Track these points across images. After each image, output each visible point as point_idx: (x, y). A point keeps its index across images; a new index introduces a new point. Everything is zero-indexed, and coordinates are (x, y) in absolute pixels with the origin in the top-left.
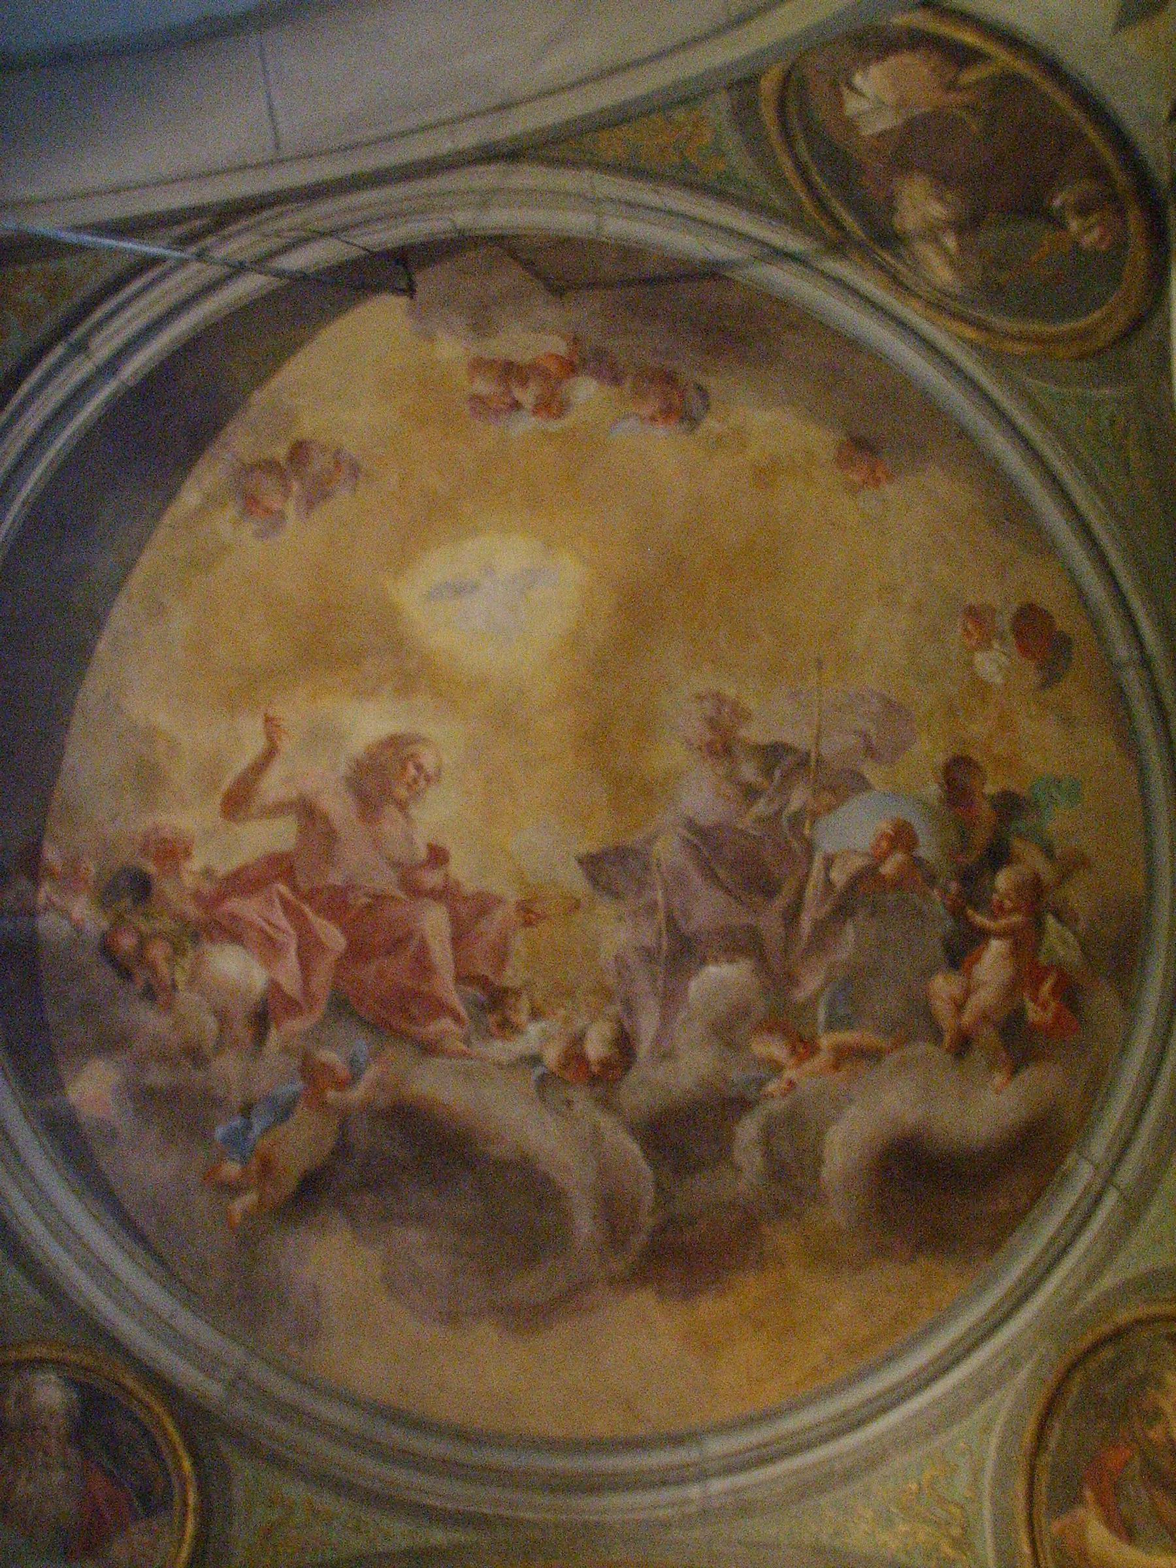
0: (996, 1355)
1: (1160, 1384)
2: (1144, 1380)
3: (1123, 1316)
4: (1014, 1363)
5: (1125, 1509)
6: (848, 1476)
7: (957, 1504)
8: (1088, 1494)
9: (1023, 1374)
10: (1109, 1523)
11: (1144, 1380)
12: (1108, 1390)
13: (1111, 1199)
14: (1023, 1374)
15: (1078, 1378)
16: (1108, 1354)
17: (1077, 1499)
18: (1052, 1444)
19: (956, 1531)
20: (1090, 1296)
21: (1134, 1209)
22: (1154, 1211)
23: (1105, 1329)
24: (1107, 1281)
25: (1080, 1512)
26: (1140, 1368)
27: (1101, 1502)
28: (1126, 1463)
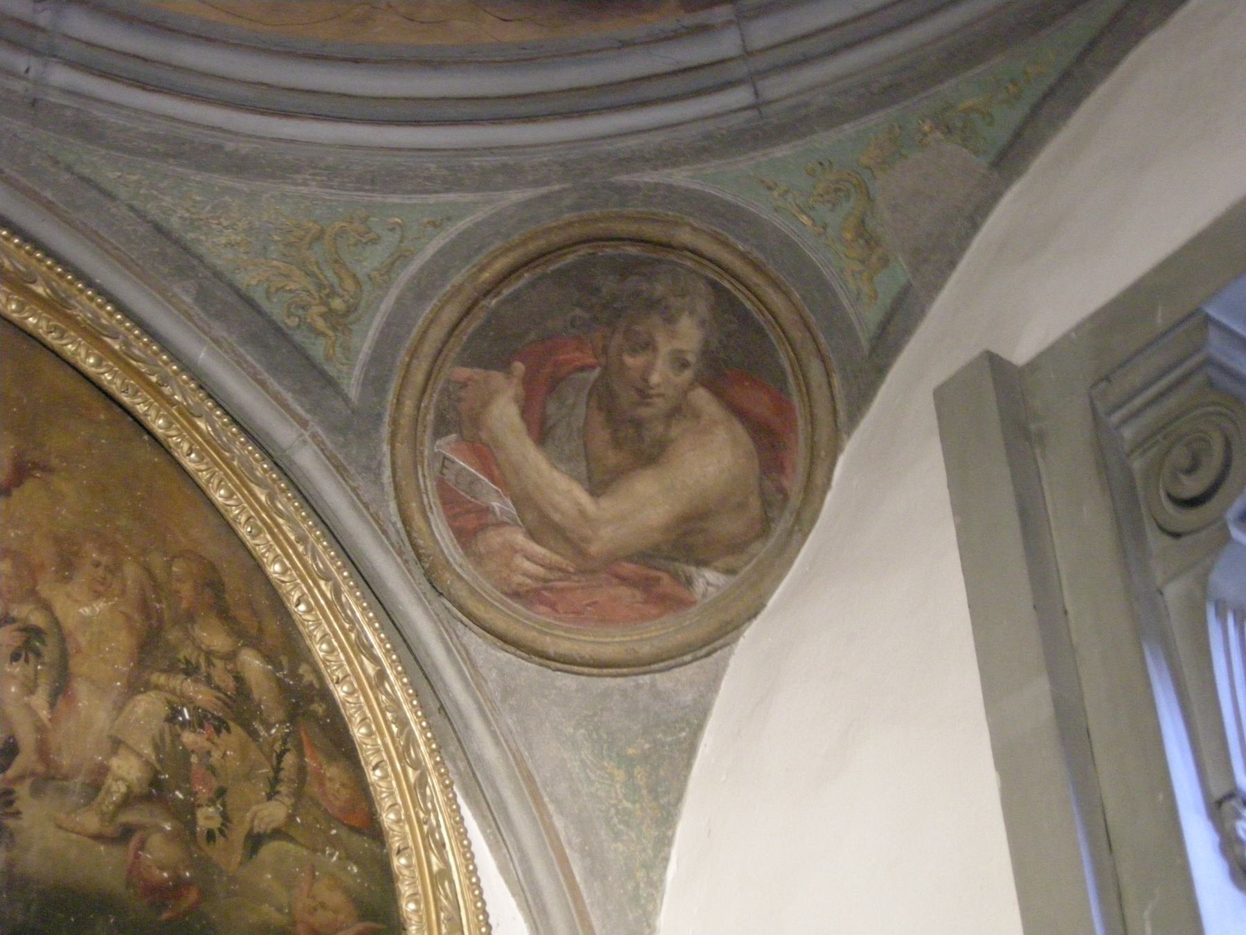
0: (490, 150)
1: (670, 320)
2: (652, 305)
3: (685, 236)
4: (512, 175)
5: (552, 408)
6: (240, 166)
7: (354, 276)
8: (519, 367)
9: (515, 196)
10: (525, 413)
11: (652, 305)
12: (608, 284)
13: (740, 96)
14: (515, 196)
15: (584, 250)
16: (632, 250)
17: (504, 366)
18: (506, 292)
19: (337, 304)
20: (649, 177)
21: (759, 132)
22: (781, 152)
23: (651, 231)
24: (680, 177)
25: (498, 378)
26: (659, 289)
27: (528, 382)
28: (582, 369)
